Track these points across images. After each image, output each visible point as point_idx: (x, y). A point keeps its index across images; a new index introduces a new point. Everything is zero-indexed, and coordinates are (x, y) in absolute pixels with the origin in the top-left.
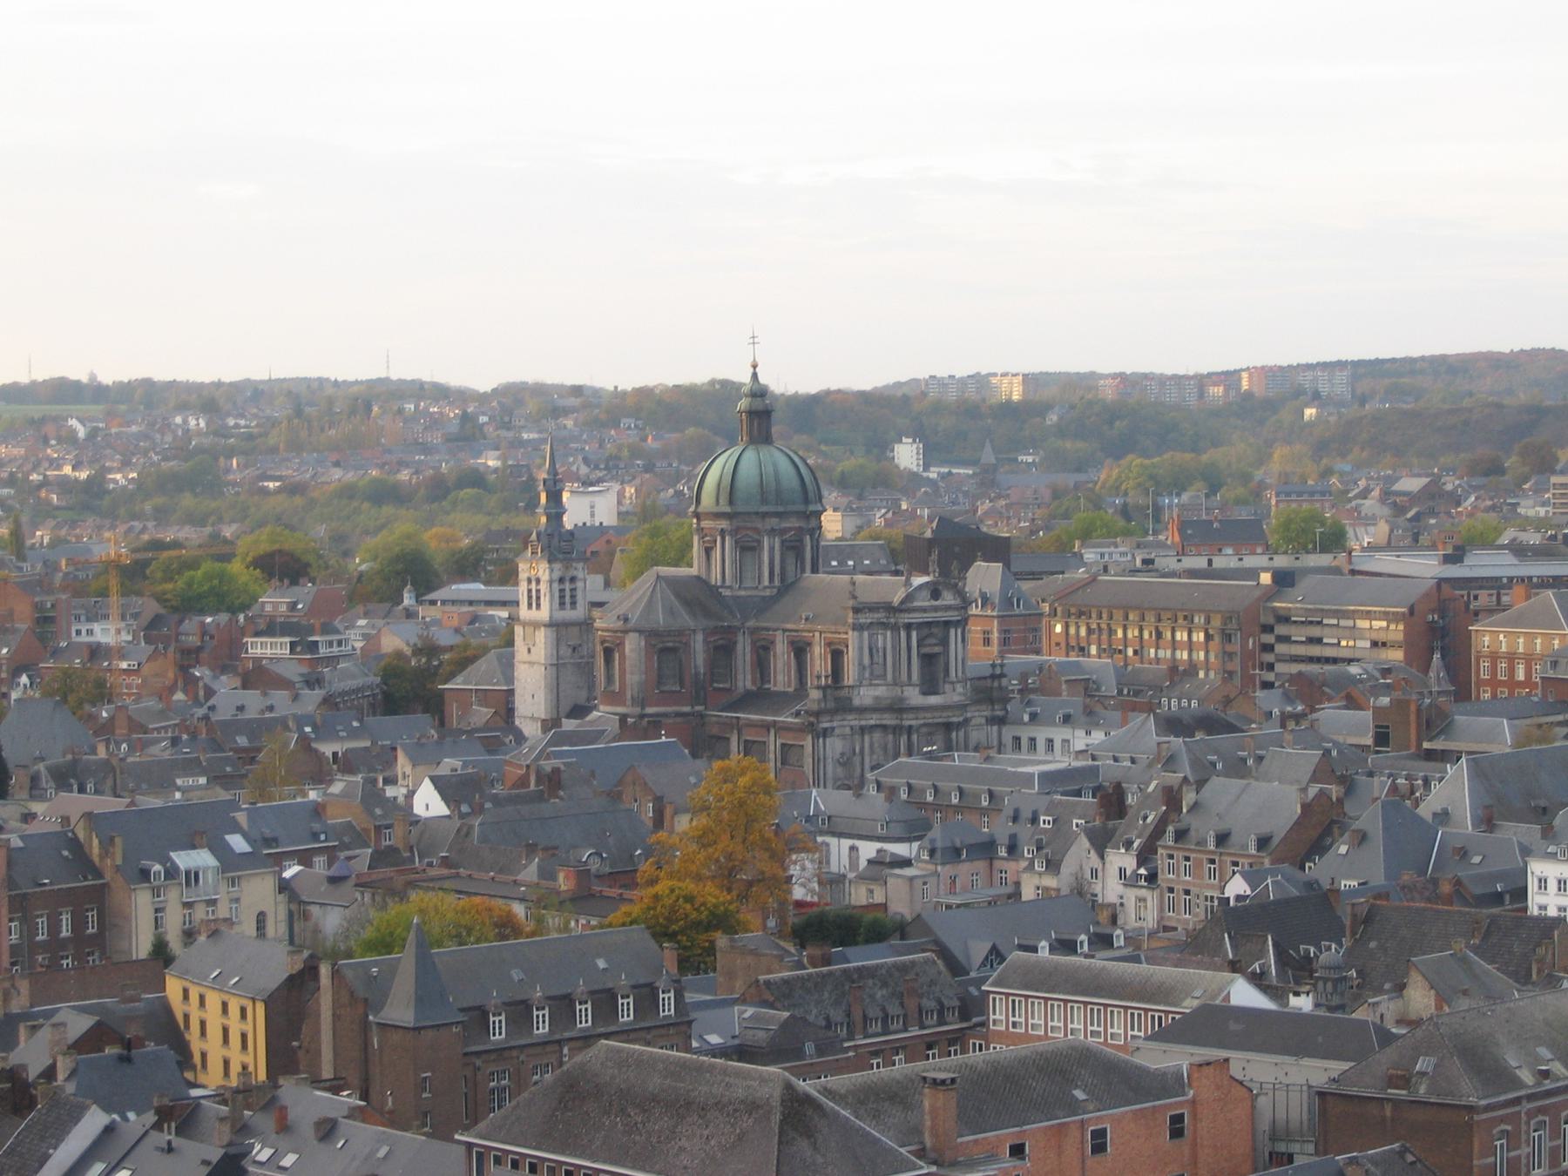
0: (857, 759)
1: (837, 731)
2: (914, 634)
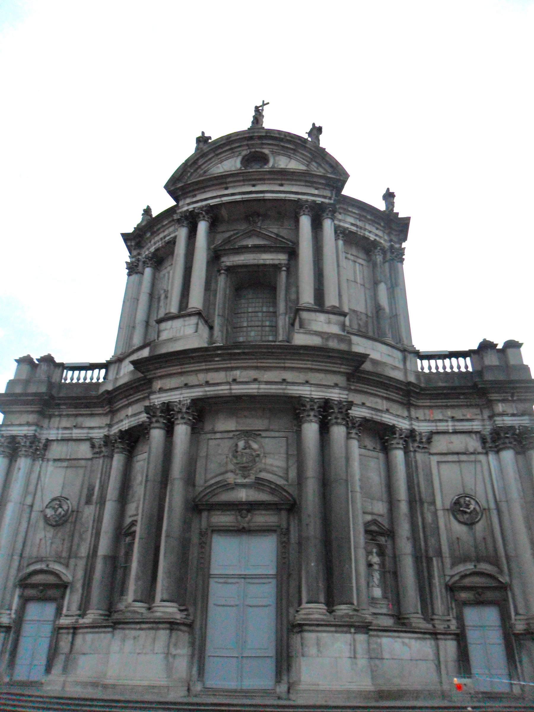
0: (89, 512)
1: (56, 450)
2: (202, 227)
